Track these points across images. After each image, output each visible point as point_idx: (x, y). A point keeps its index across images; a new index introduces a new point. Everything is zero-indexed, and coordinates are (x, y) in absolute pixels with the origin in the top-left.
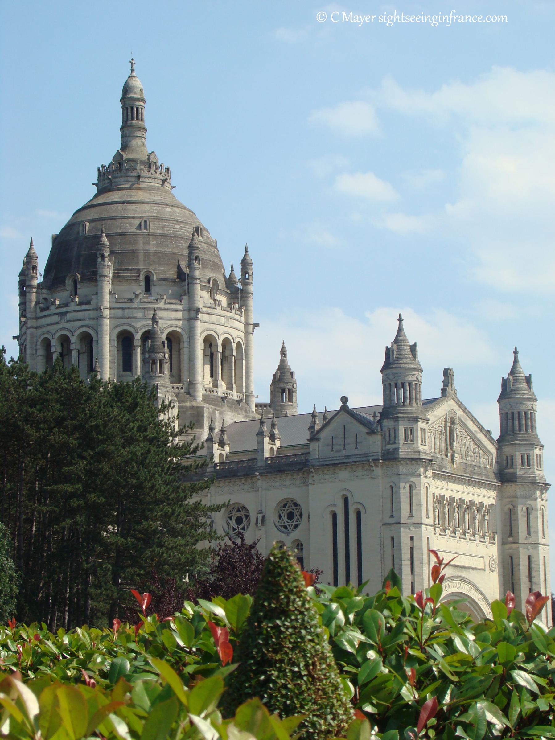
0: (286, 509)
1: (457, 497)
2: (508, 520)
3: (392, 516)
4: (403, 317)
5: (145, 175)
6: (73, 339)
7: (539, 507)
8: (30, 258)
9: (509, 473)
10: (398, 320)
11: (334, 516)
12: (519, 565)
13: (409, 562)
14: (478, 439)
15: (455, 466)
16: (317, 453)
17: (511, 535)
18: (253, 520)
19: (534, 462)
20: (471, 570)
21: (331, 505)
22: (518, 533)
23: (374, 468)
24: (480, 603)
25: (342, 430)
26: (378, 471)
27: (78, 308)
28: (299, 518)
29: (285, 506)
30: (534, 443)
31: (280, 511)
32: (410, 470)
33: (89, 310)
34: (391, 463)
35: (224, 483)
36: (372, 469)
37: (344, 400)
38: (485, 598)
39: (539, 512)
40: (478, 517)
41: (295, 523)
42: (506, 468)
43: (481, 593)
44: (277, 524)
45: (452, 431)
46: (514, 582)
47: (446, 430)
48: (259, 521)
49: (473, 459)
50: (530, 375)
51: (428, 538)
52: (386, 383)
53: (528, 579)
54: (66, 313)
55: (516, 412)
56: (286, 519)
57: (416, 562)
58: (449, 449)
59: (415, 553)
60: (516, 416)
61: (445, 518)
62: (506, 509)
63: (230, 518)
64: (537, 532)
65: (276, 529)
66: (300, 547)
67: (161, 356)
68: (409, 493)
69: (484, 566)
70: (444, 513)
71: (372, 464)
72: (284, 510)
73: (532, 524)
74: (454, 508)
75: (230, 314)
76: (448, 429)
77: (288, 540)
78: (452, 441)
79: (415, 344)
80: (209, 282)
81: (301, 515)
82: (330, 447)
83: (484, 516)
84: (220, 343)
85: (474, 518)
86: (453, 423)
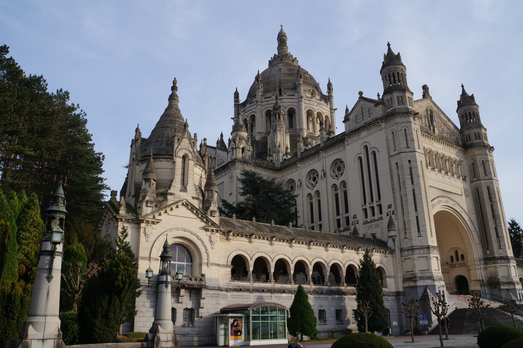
1: (440, 152)
2: (472, 169)
3: (394, 151)
4: (390, 43)
6: (248, 119)
7: (489, 160)
8: (237, 95)
9: (469, 144)
10: (388, 45)
11: (360, 159)
12: (483, 192)
13: (410, 176)
15: (436, 135)
16: (349, 127)
17: (475, 177)
18: (320, 176)
19: (482, 136)
20: (454, 194)
21: (358, 154)
23: (380, 124)
24: (462, 214)
25: (361, 110)
26: (383, 125)
27: (250, 105)
29: (336, 165)
30: (480, 126)
31: (334, 168)
32: (404, 120)
33: (254, 105)
34: (391, 117)
35: (306, 161)
36: (379, 124)
37: (361, 93)
39: (490, 162)
40: (454, 165)
41: (341, 172)
44: (333, 175)
45: (431, 116)
46: (481, 202)
47: (428, 116)
48: (323, 175)
49: (446, 135)
50: (473, 94)
51: (421, 161)
52: (384, 77)
53: (489, 200)
54: (246, 109)
55: (467, 112)
56: (337, 172)
57: (414, 176)
58: (431, 125)
59: (413, 170)
60: (468, 115)
61: (433, 162)
62: (470, 163)
63: (310, 179)
64: (490, 173)
65: (332, 178)
68: (405, 134)
70: (433, 159)
71: (379, 121)
73: (487, 169)
74: (439, 158)
75: (320, 102)
77: (338, 183)
79: (399, 53)
81: (344, 167)
82: (355, 121)
83: (458, 165)
84: (315, 113)
85: (452, 166)
86: (431, 112)
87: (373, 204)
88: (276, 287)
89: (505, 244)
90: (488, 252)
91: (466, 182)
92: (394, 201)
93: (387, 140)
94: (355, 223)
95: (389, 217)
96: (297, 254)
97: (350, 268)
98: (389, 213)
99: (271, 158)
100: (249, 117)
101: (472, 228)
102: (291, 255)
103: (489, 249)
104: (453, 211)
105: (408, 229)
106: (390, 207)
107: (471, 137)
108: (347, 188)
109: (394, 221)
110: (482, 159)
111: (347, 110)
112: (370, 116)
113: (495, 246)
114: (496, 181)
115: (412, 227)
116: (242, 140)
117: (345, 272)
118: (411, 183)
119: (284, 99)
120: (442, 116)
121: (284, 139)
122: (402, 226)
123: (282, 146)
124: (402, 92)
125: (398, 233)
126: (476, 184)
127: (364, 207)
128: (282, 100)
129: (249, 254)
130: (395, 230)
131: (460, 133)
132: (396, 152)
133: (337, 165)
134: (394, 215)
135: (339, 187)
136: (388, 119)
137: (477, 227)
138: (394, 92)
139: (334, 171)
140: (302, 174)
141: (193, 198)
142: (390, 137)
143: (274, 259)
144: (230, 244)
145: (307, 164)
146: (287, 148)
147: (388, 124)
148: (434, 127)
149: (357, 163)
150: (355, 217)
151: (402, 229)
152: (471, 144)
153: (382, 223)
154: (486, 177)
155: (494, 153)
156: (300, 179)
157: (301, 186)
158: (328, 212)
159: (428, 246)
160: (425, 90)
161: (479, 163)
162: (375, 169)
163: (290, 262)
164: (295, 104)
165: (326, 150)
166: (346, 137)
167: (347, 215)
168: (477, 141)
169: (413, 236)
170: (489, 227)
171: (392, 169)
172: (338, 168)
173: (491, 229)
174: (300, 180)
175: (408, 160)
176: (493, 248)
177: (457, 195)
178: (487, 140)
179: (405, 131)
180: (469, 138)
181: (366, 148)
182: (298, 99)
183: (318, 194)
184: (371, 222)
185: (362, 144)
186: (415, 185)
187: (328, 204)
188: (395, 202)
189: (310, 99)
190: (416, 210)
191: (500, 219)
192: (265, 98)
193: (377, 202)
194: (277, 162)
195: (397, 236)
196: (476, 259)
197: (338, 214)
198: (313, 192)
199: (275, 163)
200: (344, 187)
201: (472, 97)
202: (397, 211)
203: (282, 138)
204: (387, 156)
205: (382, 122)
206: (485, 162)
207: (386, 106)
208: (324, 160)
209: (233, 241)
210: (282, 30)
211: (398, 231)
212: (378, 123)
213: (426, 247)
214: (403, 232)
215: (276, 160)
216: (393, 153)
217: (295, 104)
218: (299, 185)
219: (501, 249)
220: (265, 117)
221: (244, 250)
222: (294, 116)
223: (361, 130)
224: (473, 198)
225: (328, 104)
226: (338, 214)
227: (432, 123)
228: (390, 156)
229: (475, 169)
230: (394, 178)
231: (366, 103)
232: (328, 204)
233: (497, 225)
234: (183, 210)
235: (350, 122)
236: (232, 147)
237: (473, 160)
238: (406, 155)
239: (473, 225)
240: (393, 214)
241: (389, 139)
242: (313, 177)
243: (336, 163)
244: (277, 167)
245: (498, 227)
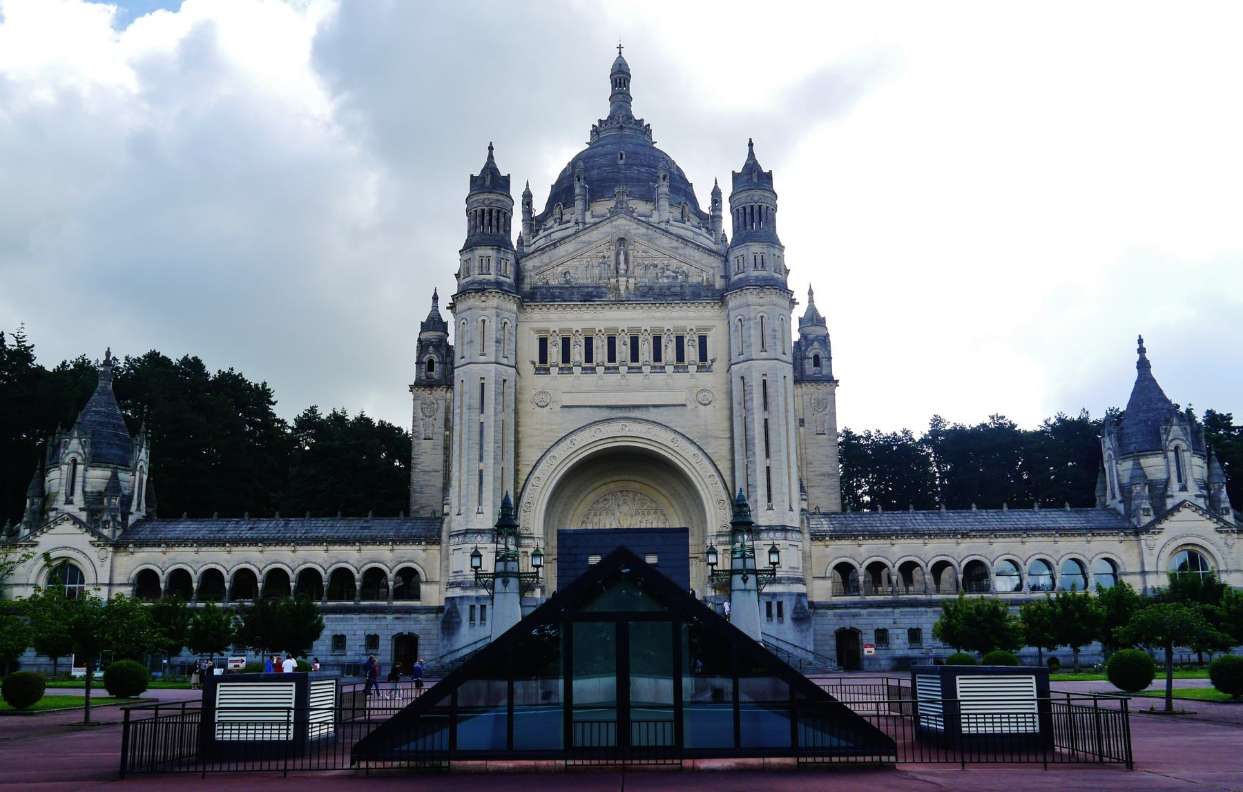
14: (680, 255)
20: (651, 409)
64: (749, 346)
89: (756, 501)
91: (712, 372)
104: (648, 442)
110: (739, 317)
116: (428, 347)
141: (81, 509)
177: (661, 409)
196: (709, 534)
210: (620, 56)
221: (153, 562)
234: (68, 527)
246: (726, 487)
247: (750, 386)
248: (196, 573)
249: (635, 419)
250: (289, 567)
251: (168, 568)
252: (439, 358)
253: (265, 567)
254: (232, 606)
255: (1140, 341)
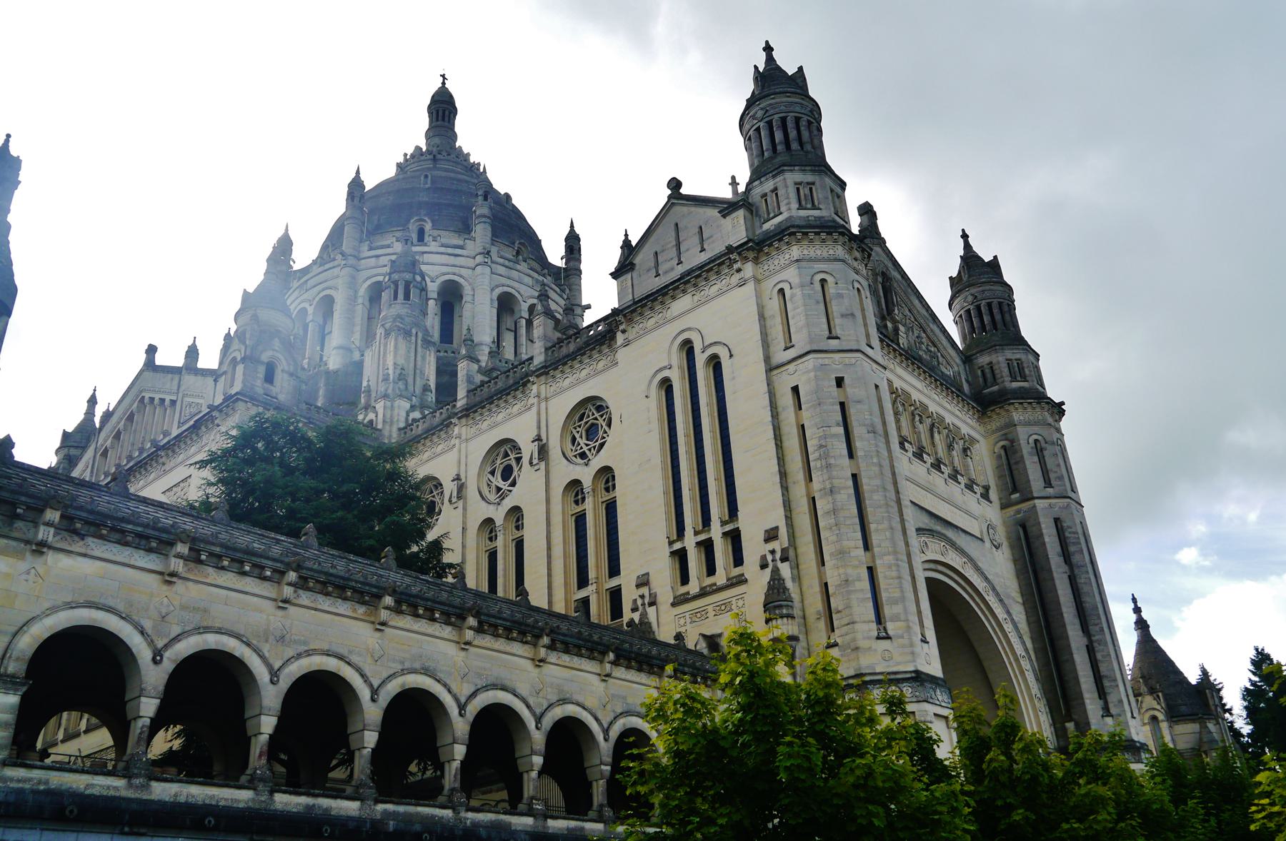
0: (583, 422)
5: (442, 158)
6: (310, 310)
9: (991, 393)
11: (666, 385)
12: (1041, 535)
13: (841, 430)
14: (932, 330)
16: (630, 290)
17: (1015, 490)
18: (525, 460)
22: (1029, 481)
26: (749, 269)
28: (607, 429)
31: (574, 431)
32: (819, 252)
33: (334, 267)
36: (736, 266)
37: (675, 184)
38: (994, 589)
41: (599, 442)
42: (986, 386)
43: (986, 579)
44: (570, 454)
51: (877, 387)
56: (583, 441)
63: (492, 473)
64: (1061, 478)
65: (566, 461)
66: (610, 484)
67: (408, 276)
68: (821, 294)
69: (981, 532)
72: (580, 426)
76: (880, 286)
77: (586, 475)
78: (891, 306)
80: (514, 243)
81: (609, 425)
82: (654, 270)
87: (710, 530)
88: (279, 806)
89: (1121, 701)
90: (1070, 726)
92: (786, 516)
93: (762, 317)
94: (643, 604)
95: (768, 571)
96: (402, 663)
97: (631, 742)
98: (769, 558)
99: (371, 416)
100: (315, 302)
101: (1019, 650)
102: (369, 660)
103: (1074, 717)
105: (839, 612)
106: (771, 535)
107: (996, 372)
108: (619, 493)
109: (789, 584)
110: (1035, 437)
111: (626, 244)
112: (705, 247)
113: (1092, 706)
114: (1079, 507)
115: (854, 603)
117: (609, 760)
118: (845, 452)
119: (432, 253)
120: (916, 302)
121: (419, 358)
122: (814, 603)
123: (410, 380)
124: (811, 171)
125: (804, 630)
126: (1018, 512)
127: (677, 546)
128: (425, 255)
129: (149, 631)
130: (793, 617)
131: (964, 363)
132: (791, 353)
133: (585, 420)
134: (786, 565)
135: (589, 490)
136: (766, 249)
137: (1029, 645)
138: (785, 168)
139: (574, 439)
140: (466, 457)
142: (774, 305)
143: (286, 670)
144: (41, 570)
145: (485, 425)
146: (426, 389)
147: (766, 267)
148: (894, 322)
149: (656, 397)
150: (643, 582)
151: (818, 613)
152: (999, 391)
153: (741, 597)
154: (1050, 490)
155: (1065, 424)
156: (458, 475)
157: (459, 498)
158: (549, 575)
159: (917, 672)
160: (865, 217)
161: (1026, 449)
162: (716, 414)
163: (364, 693)
164: (464, 272)
165: (552, 373)
166: (620, 318)
167: (614, 583)
168: (1015, 385)
169: (859, 636)
170: (1069, 646)
171: (780, 409)
172: (587, 431)
173: (1074, 651)
174: (458, 478)
175: (834, 376)
176: (1085, 711)
177: (969, 538)
178: (1042, 385)
179: (823, 287)
180: (990, 374)
181: (688, 347)
182: (474, 258)
183: (518, 520)
184: (703, 593)
185: (675, 338)
186: (860, 460)
187: (549, 548)
188: (789, 518)
189: (511, 264)
190: (867, 547)
191: (1099, 618)
192: (371, 249)
193: (723, 523)
194: (387, 427)
195: (802, 637)
197: (583, 581)
198: (499, 515)
199: (380, 430)
200: (607, 490)
201: (994, 265)
202: (795, 549)
203: (413, 354)
204: (762, 367)
205: (746, 259)
206: (1043, 442)
207: (758, 215)
208: (543, 405)
209: (61, 556)
211: (803, 621)
212: (730, 266)
213: (908, 676)
214: (822, 625)
215: (384, 421)
216: (780, 356)
217: (464, 272)
218: (455, 494)
219: (1112, 716)
220: (367, 304)
222: (457, 309)
223: (671, 293)
224: (1013, 554)
225: (563, 291)
226: (583, 581)
227: (890, 312)
228: (771, 368)
229: (1014, 467)
230: (784, 438)
231: (693, 209)
232: (549, 548)
233: (1093, 638)
235: (635, 274)
236: (234, 358)
237: (1006, 439)
238: (826, 361)
239: (1021, 637)
240: (784, 559)
241: (767, 314)
242: (502, 466)
243: (584, 414)
244: (386, 441)
245: (1095, 644)
246: (1037, 680)
247: (1074, 533)
248: (274, 676)
249: (953, 545)
250: (528, 706)
251: (177, 639)
252: (289, 364)
253: (474, 695)
254: (385, 812)
255: (1134, 600)
